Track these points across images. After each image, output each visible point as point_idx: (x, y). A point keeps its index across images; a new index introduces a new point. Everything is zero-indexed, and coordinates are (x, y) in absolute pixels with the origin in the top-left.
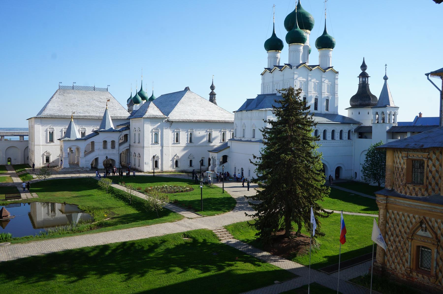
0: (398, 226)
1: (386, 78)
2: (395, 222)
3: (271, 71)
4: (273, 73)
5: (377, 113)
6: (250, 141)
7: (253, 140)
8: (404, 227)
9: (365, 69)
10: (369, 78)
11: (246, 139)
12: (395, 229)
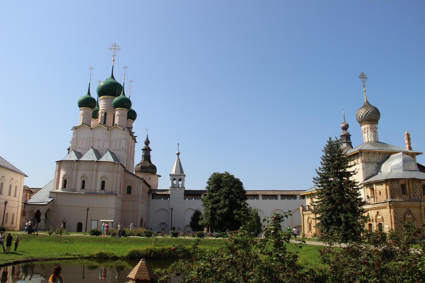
0: (399, 215)
1: (178, 154)
2: (397, 214)
3: (92, 128)
4: (92, 131)
5: (174, 179)
6: (95, 194)
8: (401, 215)
9: (148, 145)
10: (151, 151)
12: (398, 218)
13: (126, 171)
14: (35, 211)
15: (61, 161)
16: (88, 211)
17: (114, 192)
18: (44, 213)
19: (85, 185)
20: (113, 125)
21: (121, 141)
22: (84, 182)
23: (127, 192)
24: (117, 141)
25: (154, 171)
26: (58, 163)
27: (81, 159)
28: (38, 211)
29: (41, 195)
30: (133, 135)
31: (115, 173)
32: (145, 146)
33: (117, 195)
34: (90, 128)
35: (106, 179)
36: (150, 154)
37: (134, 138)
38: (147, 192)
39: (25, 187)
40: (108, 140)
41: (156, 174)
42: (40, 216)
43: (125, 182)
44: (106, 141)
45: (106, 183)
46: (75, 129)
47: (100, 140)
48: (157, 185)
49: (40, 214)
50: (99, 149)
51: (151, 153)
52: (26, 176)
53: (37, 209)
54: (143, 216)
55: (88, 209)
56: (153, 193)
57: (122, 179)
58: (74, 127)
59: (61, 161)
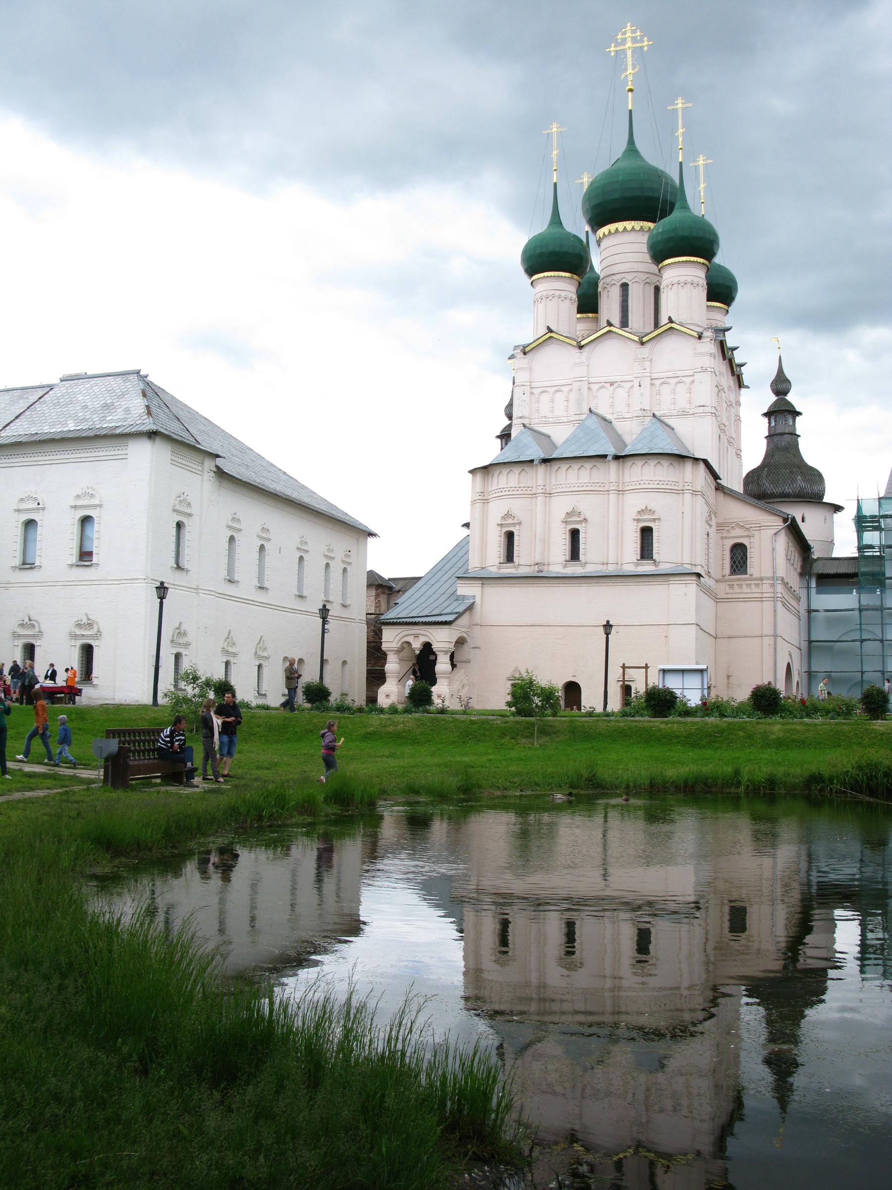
3: (583, 343)
4: (586, 350)
7: (647, 567)
9: (786, 393)
10: (798, 418)
11: (590, 569)
13: (719, 488)
14: (417, 645)
15: (485, 469)
16: (607, 634)
17: (689, 567)
18: (446, 652)
19: (582, 546)
20: (657, 325)
21: (693, 382)
22: (575, 534)
23: (732, 567)
24: (678, 379)
25: (816, 488)
26: (479, 477)
27: (554, 456)
28: (427, 647)
29: (429, 593)
30: (731, 362)
31: (688, 496)
32: (776, 402)
33: (699, 575)
34: (574, 343)
35: (654, 520)
36: (795, 429)
37: (735, 372)
38: (799, 570)
39: (371, 575)
40: (647, 381)
41: (824, 500)
42: (434, 662)
43: (720, 527)
44: (636, 384)
45: (655, 534)
46: (522, 356)
47: (616, 384)
48: (832, 543)
49: (432, 657)
50: (615, 416)
51: (801, 425)
52: (371, 534)
53: (423, 639)
54: (790, 655)
55: (608, 627)
56: (820, 572)
57: (711, 519)
58: (516, 347)
59: (490, 469)
